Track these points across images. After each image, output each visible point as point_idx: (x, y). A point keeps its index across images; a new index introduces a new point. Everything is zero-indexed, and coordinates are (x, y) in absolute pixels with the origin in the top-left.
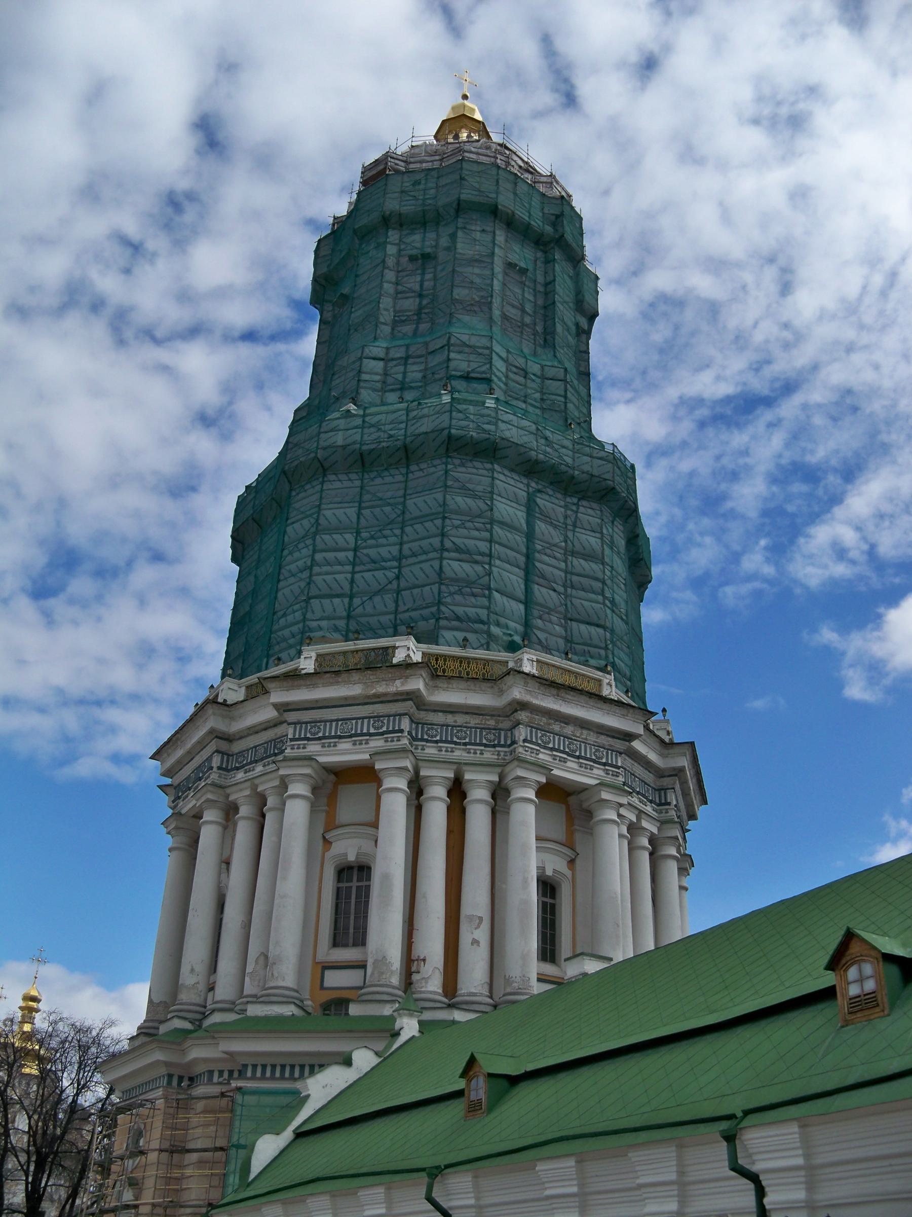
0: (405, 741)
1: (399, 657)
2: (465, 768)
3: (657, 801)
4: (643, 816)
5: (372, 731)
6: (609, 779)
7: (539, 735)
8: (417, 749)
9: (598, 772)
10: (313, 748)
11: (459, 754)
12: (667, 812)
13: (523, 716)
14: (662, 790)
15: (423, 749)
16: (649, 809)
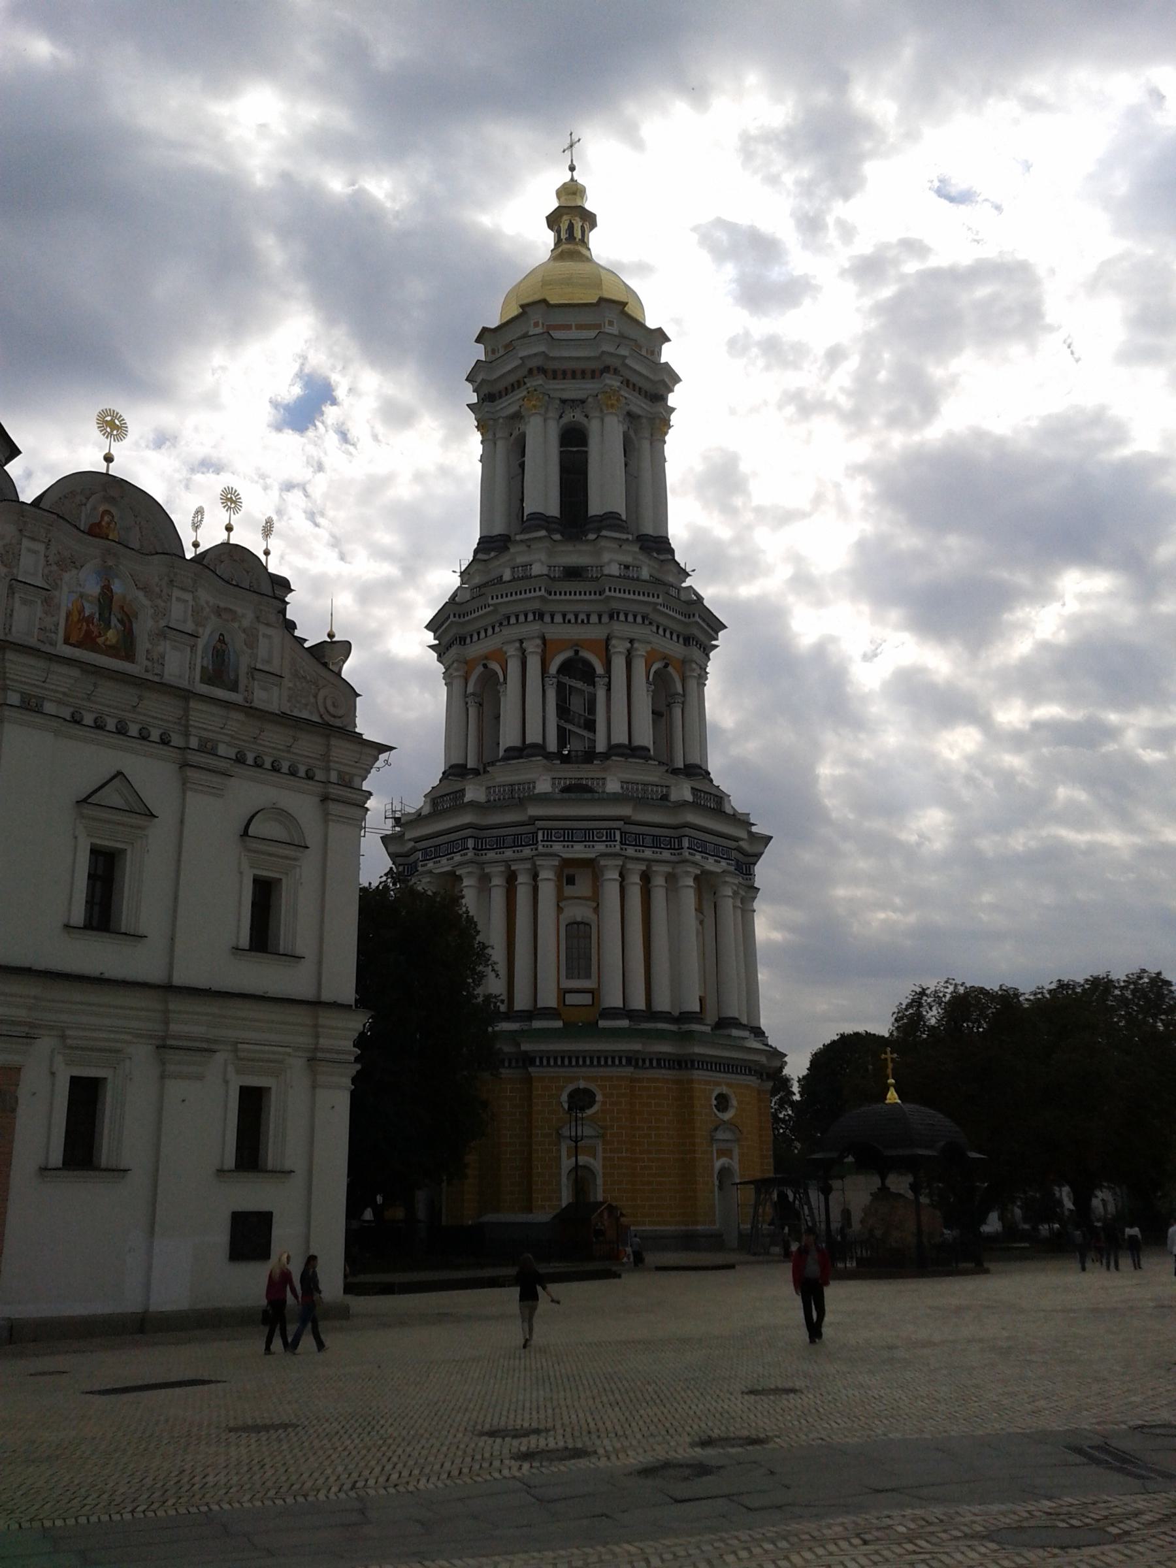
0: (470, 854)
1: (469, 797)
2: (510, 863)
3: (677, 847)
4: (653, 863)
5: (455, 850)
6: (609, 850)
7: (553, 833)
8: (482, 855)
9: (600, 847)
10: (430, 865)
11: (509, 853)
12: (681, 854)
13: (539, 824)
14: (680, 838)
15: (486, 854)
16: (666, 855)
